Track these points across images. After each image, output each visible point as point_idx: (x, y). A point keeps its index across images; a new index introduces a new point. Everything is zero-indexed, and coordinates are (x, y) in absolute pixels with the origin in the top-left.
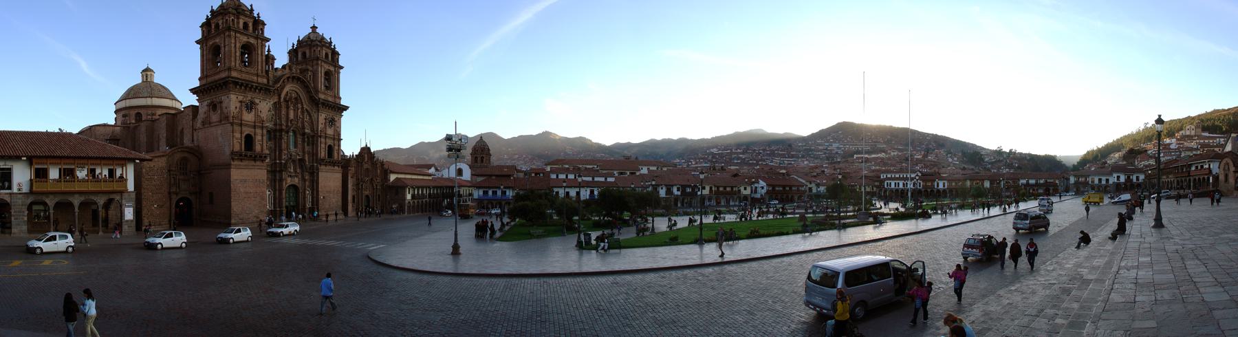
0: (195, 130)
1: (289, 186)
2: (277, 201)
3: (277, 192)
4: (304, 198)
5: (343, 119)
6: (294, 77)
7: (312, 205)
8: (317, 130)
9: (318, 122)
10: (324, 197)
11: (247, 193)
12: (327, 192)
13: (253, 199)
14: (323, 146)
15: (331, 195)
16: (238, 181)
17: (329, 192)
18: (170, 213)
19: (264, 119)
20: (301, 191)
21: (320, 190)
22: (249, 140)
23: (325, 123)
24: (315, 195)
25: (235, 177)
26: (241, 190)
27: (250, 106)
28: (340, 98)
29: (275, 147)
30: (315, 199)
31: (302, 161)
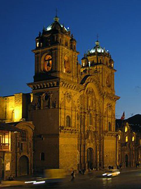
0: (30, 111)
1: (88, 149)
4: (96, 156)
7: (100, 160)
10: (107, 156)
11: (67, 153)
14: (106, 123)
15: (111, 155)
16: (63, 146)
18: (16, 166)
19: (76, 106)
21: (104, 151)
22: (69, 118)
25: (62, 143)
26: (65, 151)
27: (69, 96)
30: (101, 157)
31: (95, 132)
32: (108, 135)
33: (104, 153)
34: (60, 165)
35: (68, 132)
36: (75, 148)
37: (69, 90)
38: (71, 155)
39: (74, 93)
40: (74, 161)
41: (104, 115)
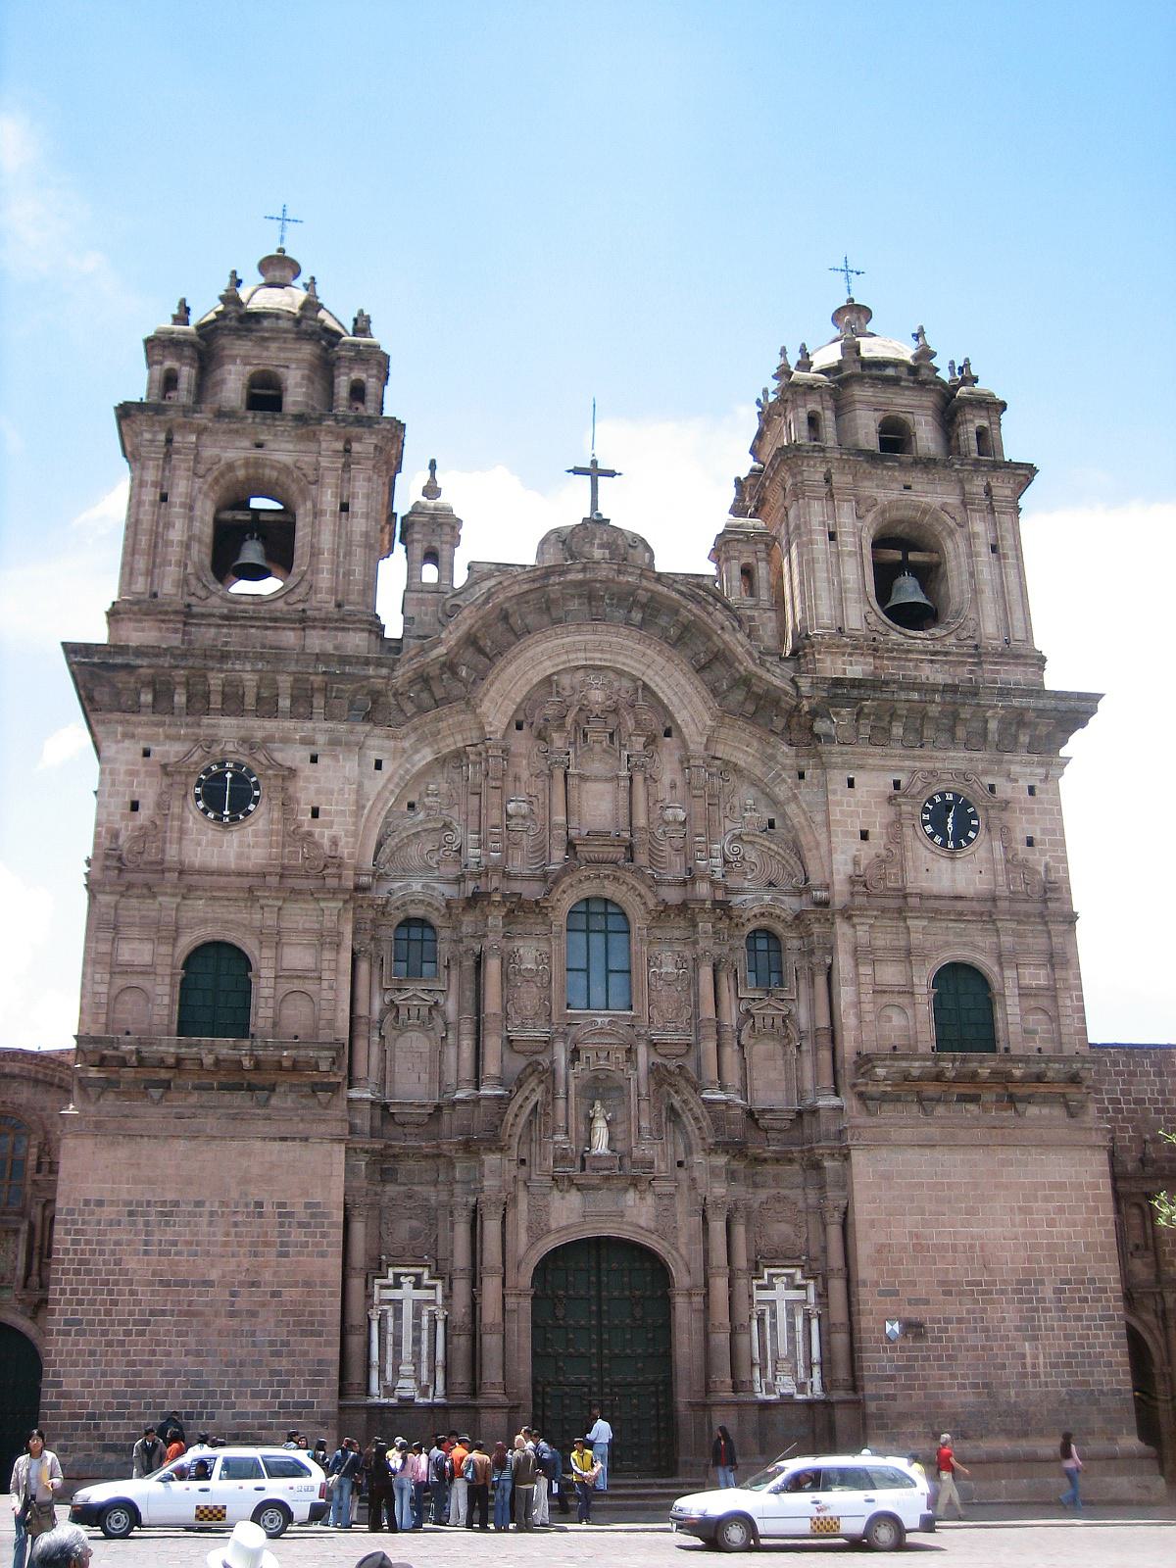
2: (462, 1342)
3: (461, 1287)
5: (1073, 786)
6: (589, 593)
8: (827, 888)
9: (828, 824)
10: (914, 1328)
12: (948, 1289)
13: (222, 1322)
14: (891, 974)
15: (1007, 1315)
16: (108, 1212)
17: (983, 1291)
20: (681, 1279)
21: (865, 1271)
23: (895, 828)
24: (838, 1315)
25: (92, 1189)
26: (132, 1263)
28: (1041, 661)
29: (460, 1011)
32: (921, 1100)
33: (864, 1294)
34: (49, 1396)
35: (196, 1088)
36: (297, 1235)
37: (228, 730)
38: (242, 1303)
39: (307, 741)
40: (284, 1364)
41: (840, 899)
